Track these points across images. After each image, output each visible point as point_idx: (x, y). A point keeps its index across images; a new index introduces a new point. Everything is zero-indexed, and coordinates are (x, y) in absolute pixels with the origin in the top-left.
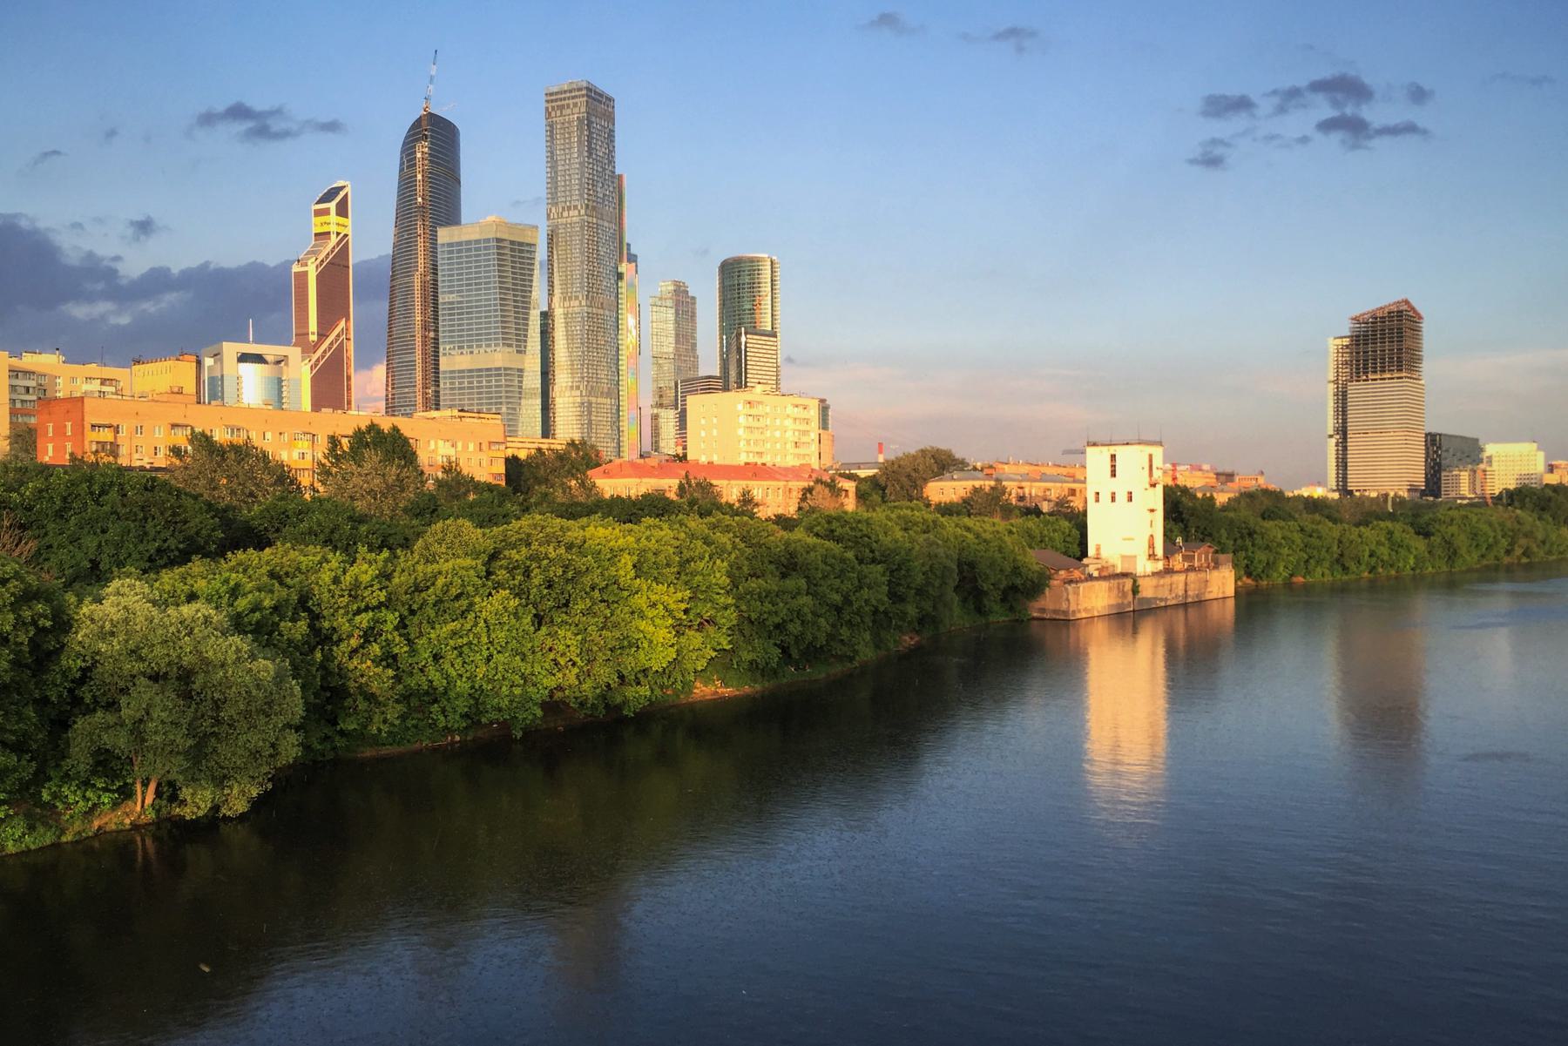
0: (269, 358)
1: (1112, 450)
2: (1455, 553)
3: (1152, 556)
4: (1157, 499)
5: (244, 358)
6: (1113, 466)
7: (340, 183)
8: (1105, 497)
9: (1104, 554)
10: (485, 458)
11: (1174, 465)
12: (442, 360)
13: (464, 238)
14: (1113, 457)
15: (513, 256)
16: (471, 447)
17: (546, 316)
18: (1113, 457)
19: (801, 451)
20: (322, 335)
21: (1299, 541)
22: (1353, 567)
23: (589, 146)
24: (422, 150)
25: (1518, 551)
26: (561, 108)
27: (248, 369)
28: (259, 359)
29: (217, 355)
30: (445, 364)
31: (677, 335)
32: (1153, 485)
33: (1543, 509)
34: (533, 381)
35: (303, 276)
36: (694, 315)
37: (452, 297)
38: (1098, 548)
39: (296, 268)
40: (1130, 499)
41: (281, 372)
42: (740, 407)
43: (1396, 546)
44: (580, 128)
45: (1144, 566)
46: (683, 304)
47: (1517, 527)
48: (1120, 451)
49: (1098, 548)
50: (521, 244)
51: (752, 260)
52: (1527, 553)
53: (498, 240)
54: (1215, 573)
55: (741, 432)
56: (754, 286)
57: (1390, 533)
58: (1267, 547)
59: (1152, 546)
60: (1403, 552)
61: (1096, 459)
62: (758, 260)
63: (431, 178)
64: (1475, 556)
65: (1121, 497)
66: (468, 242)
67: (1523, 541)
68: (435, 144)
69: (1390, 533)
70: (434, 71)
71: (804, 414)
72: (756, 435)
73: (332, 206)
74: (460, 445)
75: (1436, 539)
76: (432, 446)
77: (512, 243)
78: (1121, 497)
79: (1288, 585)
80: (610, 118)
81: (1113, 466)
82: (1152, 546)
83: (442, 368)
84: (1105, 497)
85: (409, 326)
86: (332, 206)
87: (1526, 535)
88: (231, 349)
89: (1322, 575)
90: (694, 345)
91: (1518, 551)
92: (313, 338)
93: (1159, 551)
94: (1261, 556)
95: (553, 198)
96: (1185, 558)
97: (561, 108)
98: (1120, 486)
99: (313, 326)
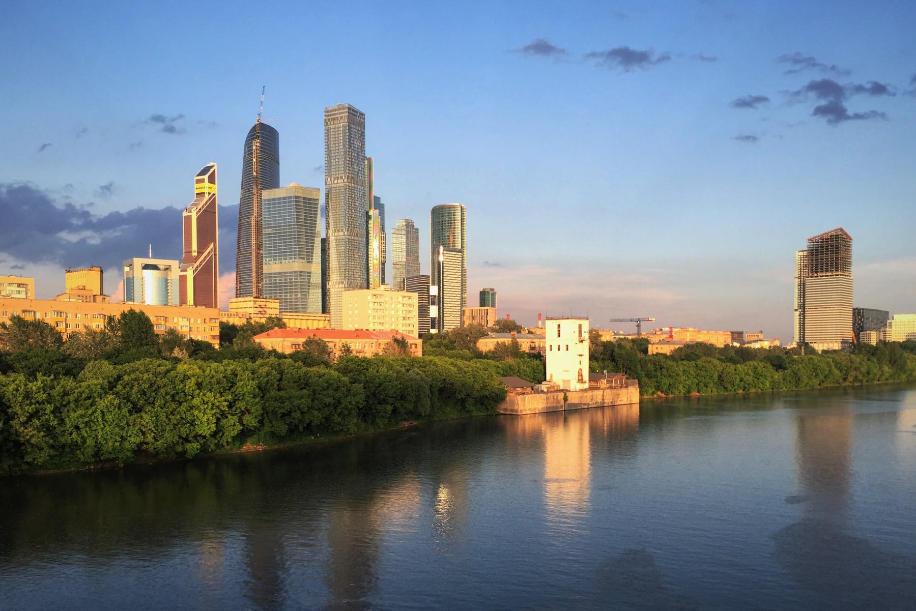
0: (161, 267)
1: (559, 322)
2: (799, 379)
3: (581, 380)
4: (585, 349)
5: (146, 267)
6: (559, 331)
8: (555, 348)
9: (554, 379)
11: (671, 328)
12: (265, 267)
13: (277, 196)
14: (559, 326)
15: (305, 206)
16: (199, 321)
17: (324, 242)
18: (559, 326)
19: (407, 322)
20: (200, 253)
21: (692, 372)
22: (730, 387)
25: (851, 379)
27: (148, 273)
28: (155, 267)
29: (131, 265)
30: (266, 269)
32: (581, 341)
33: (873, 354)
35: (189, 218)
38: (551, 376)
40: (567, 349)
41: (167, 275)
42: (369, 298)
43: (757, 375)
45: (575, 386)
47: (849, 364)
48: (563, 323)
49: (551, 376)
52: (856, 379)
54: (624, 390)
55: (370, 311)
57: (756, 368)
58: (670, 376)
59: (580, 374)
60: (762, 379)
61: (551, 326)
64: (816, 381)
65: (563, 348)
67: (853, 373)
69: (756, 368)
71: (410, 302)
72: (380, 313)
74: (192, 320)
75: (788, 372)
76: (175, 320)
78: (563, 348)
79: (687, 398)
81: (559, 331)
82: (580, 374)
83: (264, 272)
84: (555, 348)
85: (249, 247)
87: (856, 369)
88: (138, 262)
89: (712, 392)
91: (851, 379)
92: (195, 254)
93: (586, 377)
94: (666, 381)
96: (608, 382)
98: (562, 341)
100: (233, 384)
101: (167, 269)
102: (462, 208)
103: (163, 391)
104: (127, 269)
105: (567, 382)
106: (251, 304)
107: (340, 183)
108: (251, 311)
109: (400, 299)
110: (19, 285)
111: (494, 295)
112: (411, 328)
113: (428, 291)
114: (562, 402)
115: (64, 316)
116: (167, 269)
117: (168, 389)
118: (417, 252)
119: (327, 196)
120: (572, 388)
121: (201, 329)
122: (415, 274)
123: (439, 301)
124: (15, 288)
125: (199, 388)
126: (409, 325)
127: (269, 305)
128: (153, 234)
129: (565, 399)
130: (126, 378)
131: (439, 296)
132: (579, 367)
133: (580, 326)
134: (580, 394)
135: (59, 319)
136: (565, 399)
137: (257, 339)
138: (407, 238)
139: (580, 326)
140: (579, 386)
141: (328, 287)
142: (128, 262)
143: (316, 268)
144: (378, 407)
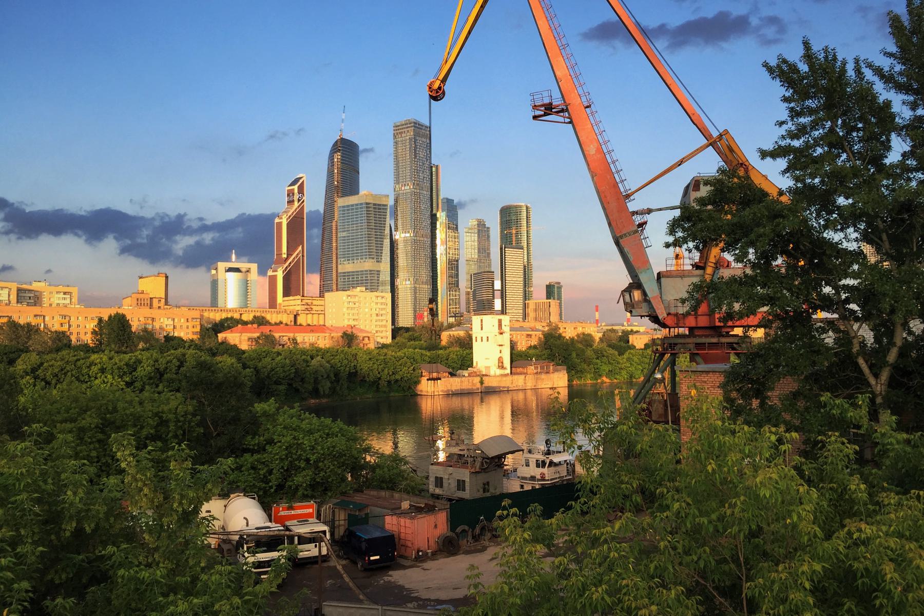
0: (243, 270)
3: (501, 366)
5: (230, 270)
8: (479, 339)
9: (479, 365)
10: (190, 324)
15: (376, 211)
16: (182, 320)
19: (380, 318)
20: (289, 255)
23: (415, 153)
24: (337, 157)
28: (237, 270)
29: (216, 269)
31: (479, 249)
34: (386, 276)
35: (280, 224)
36: (489, 237)
37: (344, 234)
39: (277, 220)
41: (247, 276)
44: (410, 144)
45: (495, 371)
46: (482, 230)
50: (379, 205)
51: (516, 207)
53: (367, 204)
55: (345, 310)
56: (518, 222)
58: (610, 363)
59: (500, 361)
62: (521, 206)
63: (342, 171)
65: (485, 339)
66: (352, 205)
68: (346, 154)
70: (343, 116)
71: (384, 300)
72: (355, 311)
73: (296, 188)
74: (176, 320)
77: (375, 204)
78: (485, 339)
82: (500, 361)
84: (479, 339)
85: (331, 248)
86: (296, 188)
88: (222, 266)
90: (489, 254)
92: (285, 256)
95: (397, 181)
100: (135, 370)
101: (248, 271)
103: (69, 374)
104: (214, 272)
105: (488, 368)
106: (299, 302)
107: (408, 188)
108: (298, 308)
109: (374, 299)
110: (65, 293)
111: (560, 288)
112: (384, 323)
113: (493, 285)
114: (479, 385)
115: (67, 319)
116: (248, 271)
117: (74, 372)
118: (489, 249)
119: (396, 201)
120: (492, 373)
121: (185, 326)
122: (487, 269)
123: (502, 295)
124: (61, 295)
125: (103, 373)
126: (382, 320)
127: (315, 302)
128: (249, 238)
129: (482, 382)
130: (45, 364)
131: (502, 290)
132: (500, 355)
133: (500, 321)
134: (498, 379)
135: (63, 321)
136: (482, 382)
137: (221, 336)
139: (500, 321)
140: (499, 372)
141: (396, 284)
142: (214, 266)
143: (385, 266)
144: (274, 387)
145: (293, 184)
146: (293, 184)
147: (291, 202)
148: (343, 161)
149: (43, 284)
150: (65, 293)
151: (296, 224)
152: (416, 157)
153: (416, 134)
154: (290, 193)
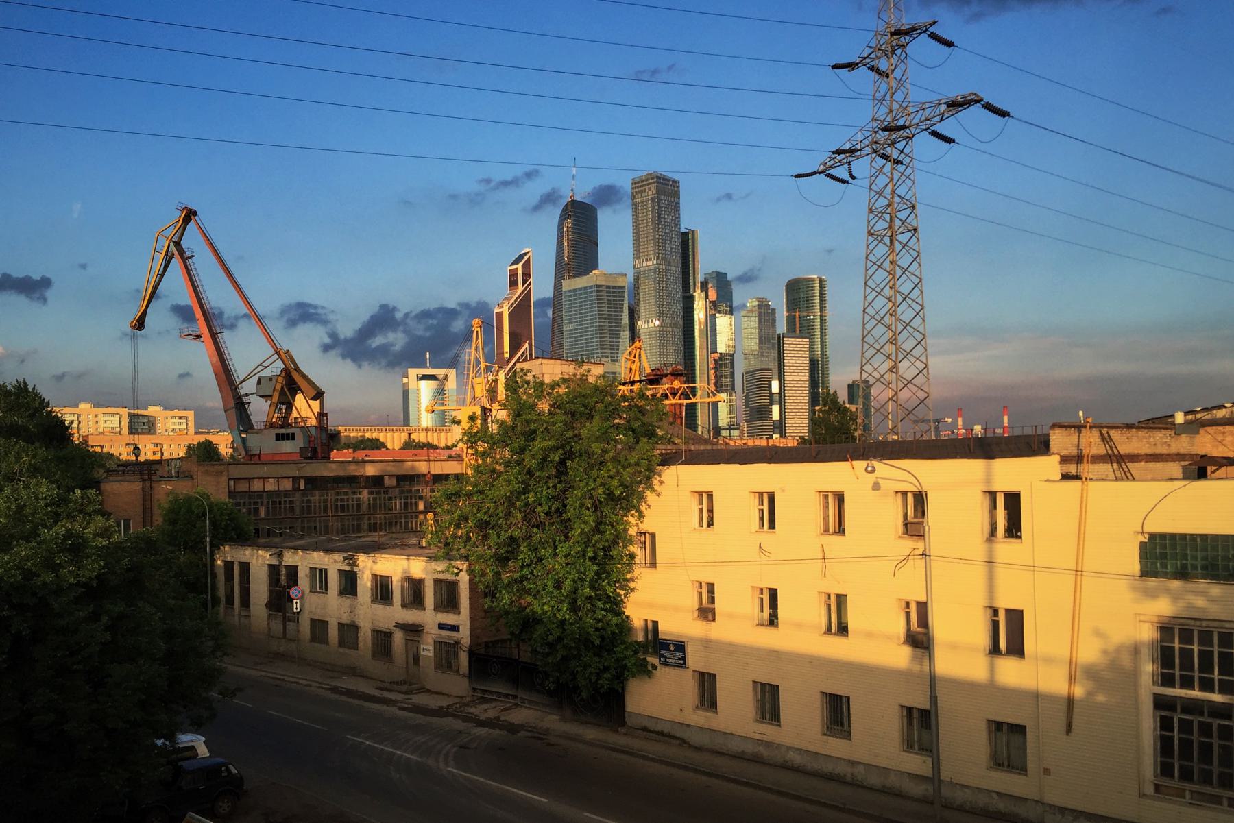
0: (441, 377)
5: (424, 377)
7: (527, 250)
15: (610, 294)
23: (659, 214)
24: (568, 224)
26: (641, 192)
27: (424, 383)
28: (433, 378)
35: (500, 315)
37: (571, 327)
39: (497, 310)
44: (653, 207)
46: (765, 313)
50: (614, 287)
53: (598, 286)
56: (809, 299)
62: (813, 280)
63: (574, 244)
73: (519, 266)
77: (608, 287)
80: (676, 194)
86: (519, 266)
88: (413, 372)
92: (507, 355)
95: (637, 254)
97: (641, 192)
99: (507, 348)
102: (821, 281)
110: (180, 418)
119: (637, 279)
124: (177, 420)
131: (780, 393)
138: (760, 322)
145: (516, 262)
146: (516, 262)
147: (514, 284)
148: (575, 230)
149: (157, 408)
150: (180, 418)
151: (521, 310)
152: (660, 222)
153: (661, 192)
154: (513, 274)
